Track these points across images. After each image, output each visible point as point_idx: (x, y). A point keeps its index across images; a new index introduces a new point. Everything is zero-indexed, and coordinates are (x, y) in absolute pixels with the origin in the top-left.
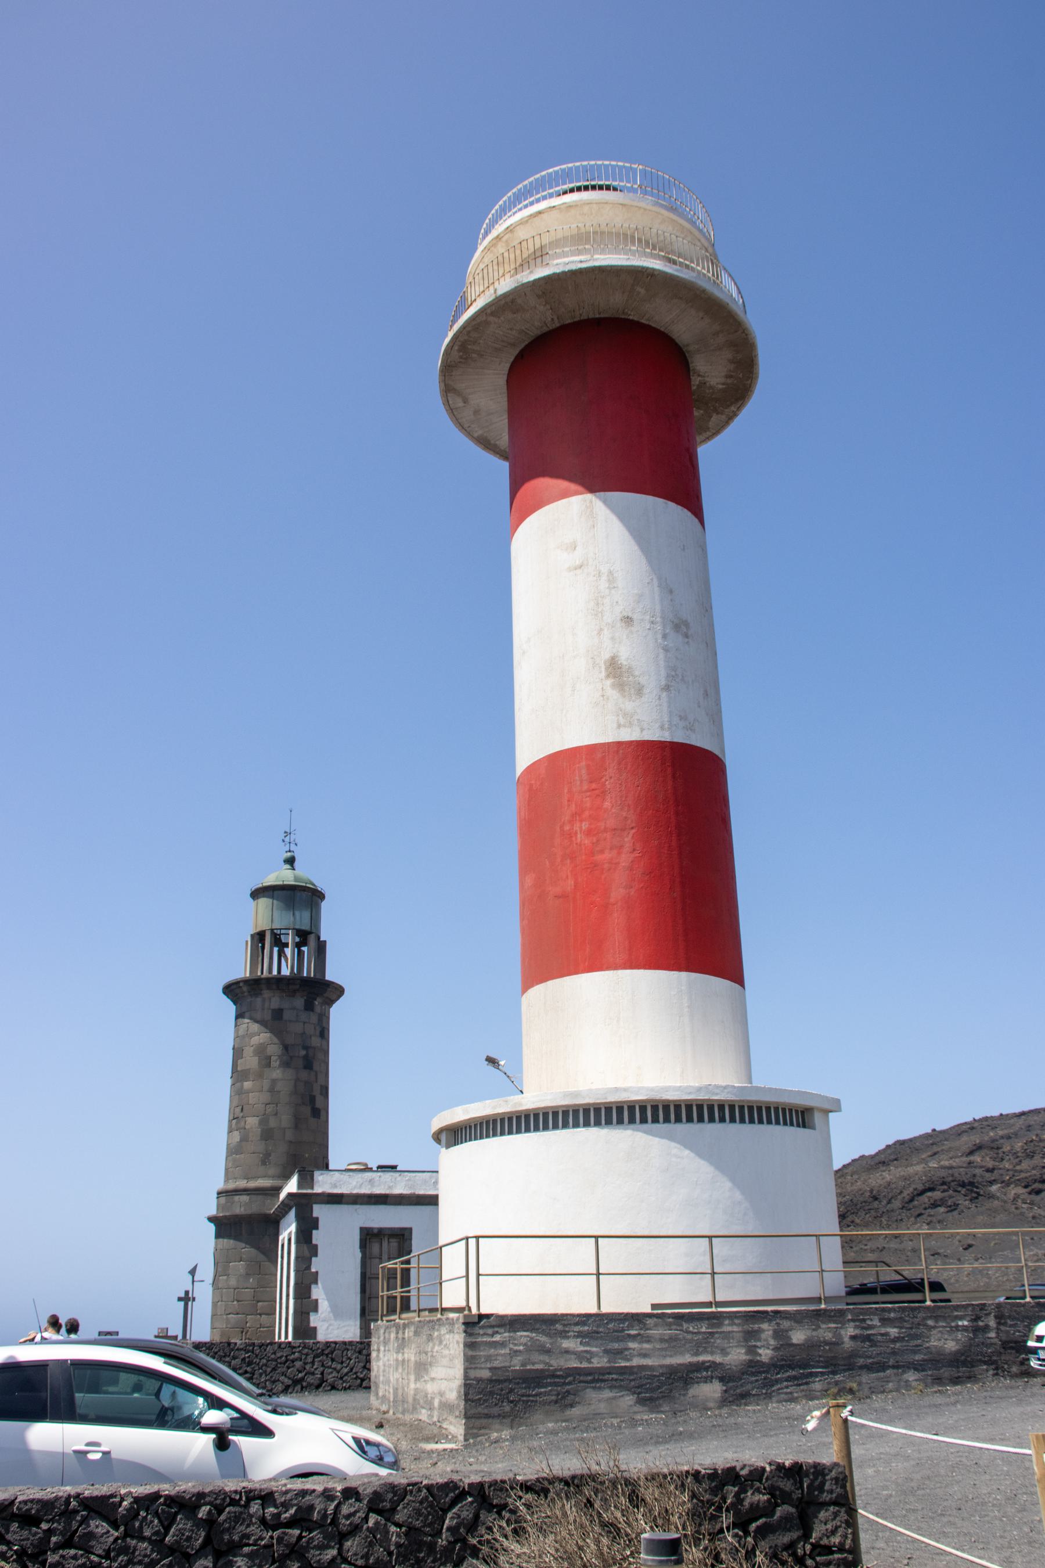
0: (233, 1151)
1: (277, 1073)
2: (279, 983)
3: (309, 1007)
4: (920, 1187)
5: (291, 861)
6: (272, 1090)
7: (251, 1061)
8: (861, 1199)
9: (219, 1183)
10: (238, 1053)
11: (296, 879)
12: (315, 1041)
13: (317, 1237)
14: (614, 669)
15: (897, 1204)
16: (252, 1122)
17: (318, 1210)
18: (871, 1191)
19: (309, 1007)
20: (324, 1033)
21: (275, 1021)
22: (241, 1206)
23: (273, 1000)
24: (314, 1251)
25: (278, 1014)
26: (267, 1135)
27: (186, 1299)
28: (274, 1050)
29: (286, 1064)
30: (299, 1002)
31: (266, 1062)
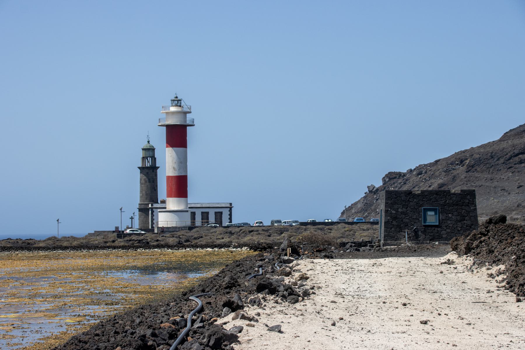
0: (141, 197)
1: (148, 184)
2: (147, 168)
3: (153, 171)
4: (516, 151)
5: (149, 142)
6: (147, 187)
7: (143, 181)
8: (485, 157)
9: (139, 202)
10: (141, 180)
11: (150, 147)
12: (155, 177)
13: (154, 213)
14: (174, 168)
15: (502, 161)
16: (144, 192)
17: (154, 210)
18: (492, 153)
19: (153, 171)
20: (156, 175)
21: (147, 175)
22: (143, 207)
23: (147, 171)
24: (154, 216)
25: (147, 173)
26: (147, 194)
27: (132, 218)
28: (147, 180)
29: (150, 182)
30: (151, 171)
31: (146, 182)
